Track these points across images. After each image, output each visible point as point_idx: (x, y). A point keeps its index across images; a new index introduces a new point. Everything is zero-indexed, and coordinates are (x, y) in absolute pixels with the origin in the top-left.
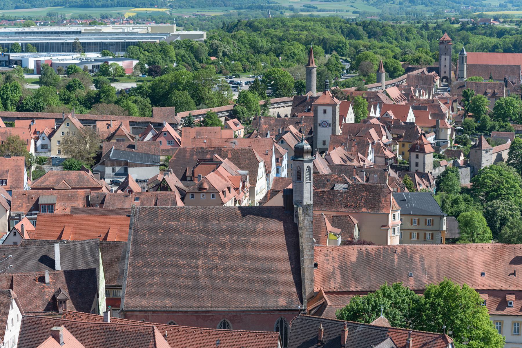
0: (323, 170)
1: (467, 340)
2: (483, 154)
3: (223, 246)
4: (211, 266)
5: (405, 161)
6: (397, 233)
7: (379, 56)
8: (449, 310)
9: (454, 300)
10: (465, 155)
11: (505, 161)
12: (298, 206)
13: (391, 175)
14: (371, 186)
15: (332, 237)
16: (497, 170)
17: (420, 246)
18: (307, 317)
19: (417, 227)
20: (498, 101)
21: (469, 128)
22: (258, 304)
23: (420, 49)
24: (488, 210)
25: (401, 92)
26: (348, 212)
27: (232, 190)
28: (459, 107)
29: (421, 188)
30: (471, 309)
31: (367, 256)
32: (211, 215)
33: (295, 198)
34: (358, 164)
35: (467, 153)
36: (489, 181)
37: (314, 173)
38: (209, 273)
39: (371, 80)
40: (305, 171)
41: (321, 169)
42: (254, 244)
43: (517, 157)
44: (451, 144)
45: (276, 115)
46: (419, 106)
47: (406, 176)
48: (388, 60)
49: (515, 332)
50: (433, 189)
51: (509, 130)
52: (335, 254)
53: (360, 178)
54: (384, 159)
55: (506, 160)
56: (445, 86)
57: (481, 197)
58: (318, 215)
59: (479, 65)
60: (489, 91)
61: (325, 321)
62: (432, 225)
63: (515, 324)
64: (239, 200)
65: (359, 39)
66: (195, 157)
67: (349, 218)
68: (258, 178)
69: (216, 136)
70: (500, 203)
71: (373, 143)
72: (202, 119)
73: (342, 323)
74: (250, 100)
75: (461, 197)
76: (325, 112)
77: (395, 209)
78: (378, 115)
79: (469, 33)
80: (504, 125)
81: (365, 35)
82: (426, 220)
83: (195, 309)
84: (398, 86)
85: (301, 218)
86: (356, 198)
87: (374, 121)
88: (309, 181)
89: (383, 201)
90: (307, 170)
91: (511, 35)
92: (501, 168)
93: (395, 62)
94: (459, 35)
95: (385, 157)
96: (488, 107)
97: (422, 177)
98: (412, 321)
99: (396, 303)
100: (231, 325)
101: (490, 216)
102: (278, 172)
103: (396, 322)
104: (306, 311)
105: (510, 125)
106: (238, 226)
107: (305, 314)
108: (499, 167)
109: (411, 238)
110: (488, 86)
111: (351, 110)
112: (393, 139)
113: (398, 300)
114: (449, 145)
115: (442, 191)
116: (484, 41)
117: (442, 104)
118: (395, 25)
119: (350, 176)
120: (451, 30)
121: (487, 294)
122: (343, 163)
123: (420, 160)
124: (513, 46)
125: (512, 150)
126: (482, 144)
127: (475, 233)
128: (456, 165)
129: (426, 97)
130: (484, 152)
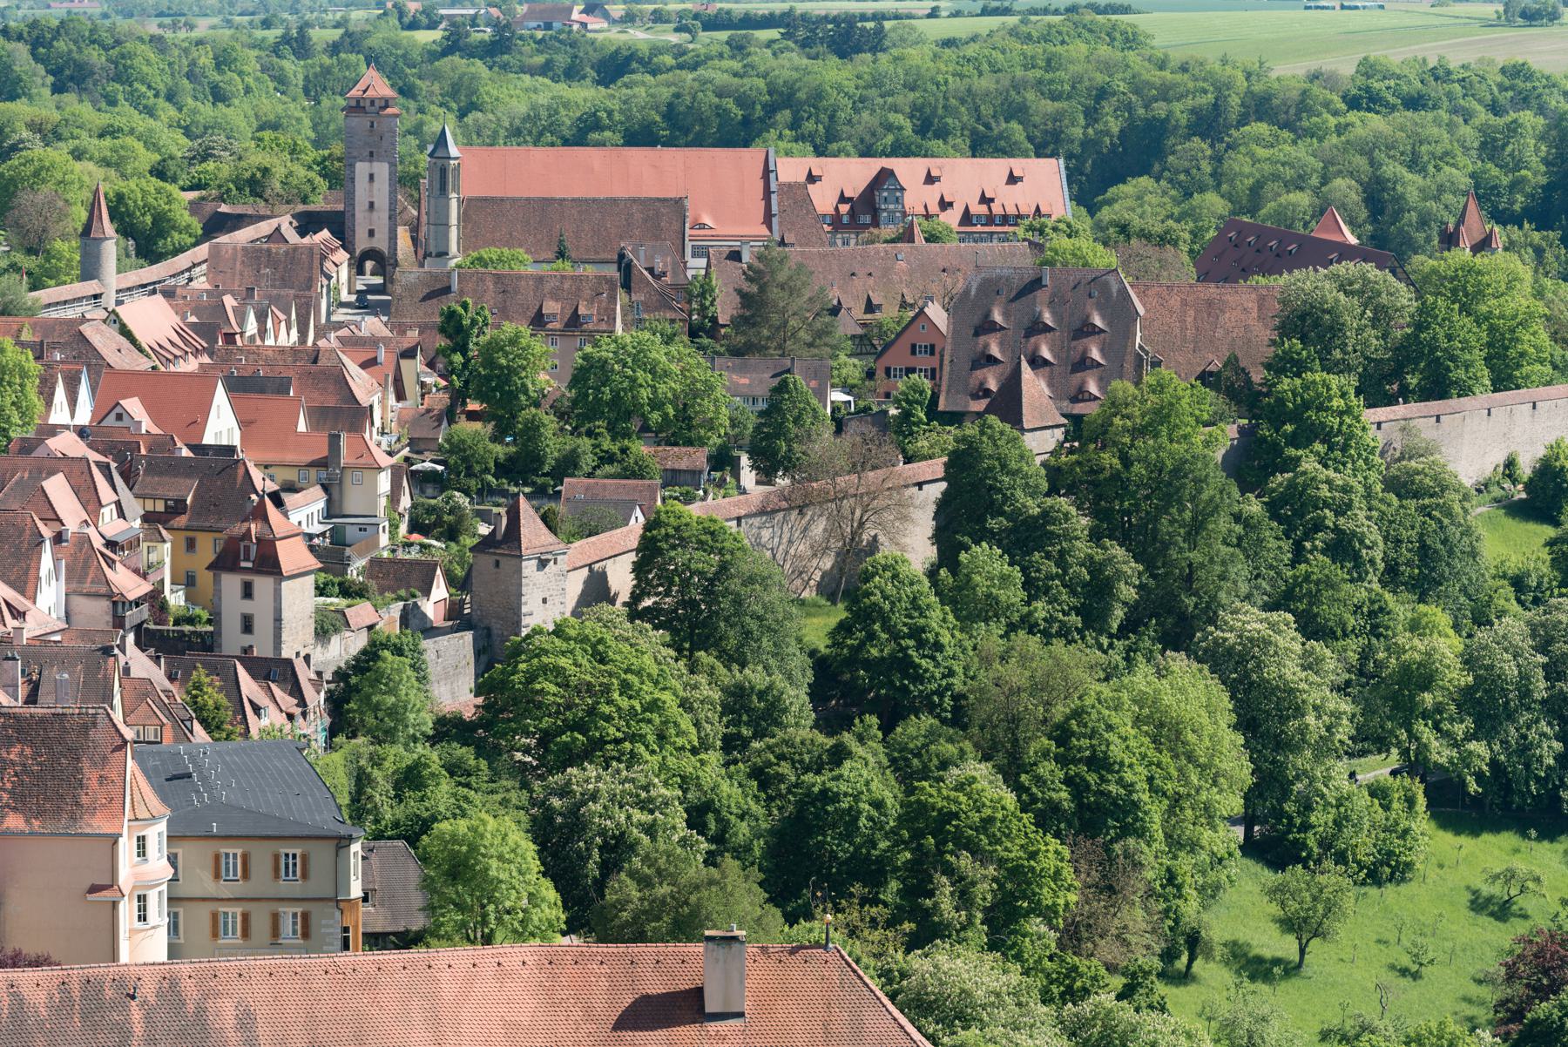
2: (525, 572)
5: (198, 611)
7: (91, 166)
10: (451, 580)
14: (43, 720)
16: (583, 639)
17: (235, 963)
19: (239, 888)
21: (469, 468)
23: (267, 135)
25: (184, 318)
28: (428, 380)
29: (265, 722)
35: (459, 572)
36: (553, 688)
39: (58, 270)
43: (672, 583)
44: (393, 535)
47: (200, 674)
48: (131, 187)
50: (315, 726)
51: (636, 472)
54: (105, 604)
55: (624, 596)
56: (372, 289)
57: (518, 756)
59: (514, 200)
60: (551, 307)
62: (305, 876)
65: (13, 97)
71: (58, 539)
75: (434, 757)
78: (84, 416)
79: (479, 67)
80: (615, 448)
81: (39, 79)
84: (169, 294)
87: (66, 444)
89: (94, 783)
91: (654, 73)
93: (158, 191)
94: (436, 76)
96: (546, 375)
97: (267, 678)
101: (558, 840)
105: (641, 448)
108: (592, 628)
109: (215, 935)
110: (548, 287)
112: (148, 518)
114: (384, 540)
115: (354, 736)
116: (543, 99)
118: (169, 35)
120: (404, 56)
123: (260, 607)
124: (664, 117)
125: (649, 554)
126: (525, 531)
127: (491, 908)
128: (414, 622)
129: (287, 338)
130: (529, 567)
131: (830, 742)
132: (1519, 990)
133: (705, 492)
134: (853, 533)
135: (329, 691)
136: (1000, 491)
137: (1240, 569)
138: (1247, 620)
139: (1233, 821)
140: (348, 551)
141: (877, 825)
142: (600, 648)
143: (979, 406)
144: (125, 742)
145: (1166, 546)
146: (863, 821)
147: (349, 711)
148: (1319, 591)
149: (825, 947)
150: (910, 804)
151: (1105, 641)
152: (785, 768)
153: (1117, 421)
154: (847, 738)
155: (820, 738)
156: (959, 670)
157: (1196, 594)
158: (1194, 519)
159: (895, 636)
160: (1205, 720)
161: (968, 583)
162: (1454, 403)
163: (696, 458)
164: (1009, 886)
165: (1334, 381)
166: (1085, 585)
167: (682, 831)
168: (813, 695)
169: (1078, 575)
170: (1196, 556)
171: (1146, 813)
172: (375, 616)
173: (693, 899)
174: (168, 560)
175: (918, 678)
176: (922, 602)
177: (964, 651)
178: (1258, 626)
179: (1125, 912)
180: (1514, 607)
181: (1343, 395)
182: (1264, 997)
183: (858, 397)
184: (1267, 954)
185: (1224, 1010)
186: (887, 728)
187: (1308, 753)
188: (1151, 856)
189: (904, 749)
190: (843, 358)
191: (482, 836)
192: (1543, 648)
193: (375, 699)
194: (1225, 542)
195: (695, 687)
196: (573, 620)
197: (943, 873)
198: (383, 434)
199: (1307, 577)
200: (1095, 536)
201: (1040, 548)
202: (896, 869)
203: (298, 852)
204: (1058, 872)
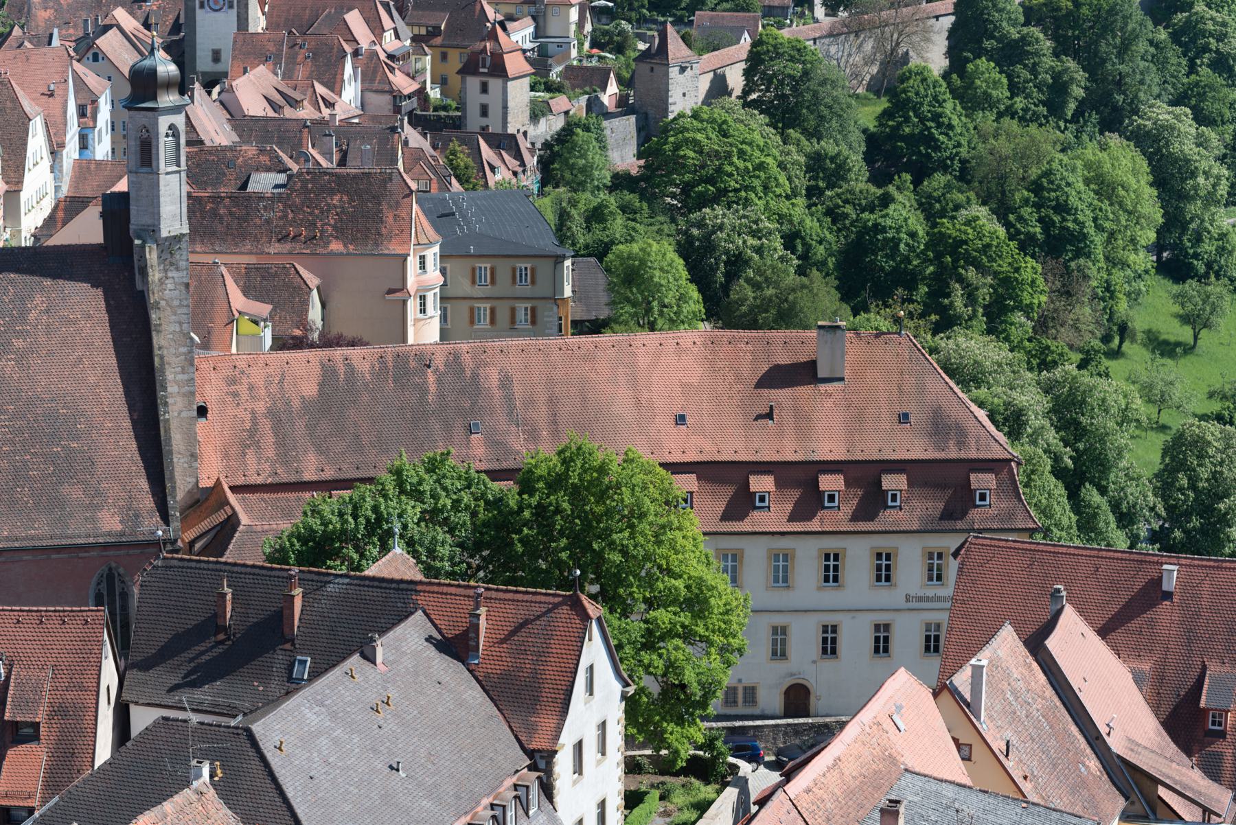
0: (213, 134)
1: (643, 607)
2: (671, 75)
5: (449, 101)
6: (433, 310)
8: (587, 526)
9: (602, 496)
10: (620, 81)
11: (735, 94)
12: (144, 242)
13: (412, 144)
14: (355, 177)
15: (246, 327)
16: (712, 121)
17: (497, 343)
18: (181, 560)
19: (488, 291)
22: (39, 530)
26: (290, 253)
29: (498, 177)
30: (651, 518)
31: (347, 379)
33: (137, 219)
35: (627, 75)
36: (692, 154)
37: (189, 143)
41: (208, 132)
43: (770, 82)
44: (579, 51)
47: (455, 145)
49: (776, 580)
50: (531, 180)
52: (257, 376)
53: (323, 154)
54: (388, 98)
55: (738, 92)
58: (203, 265)
61: (237, 572)
62: (533, 282)
63: (777, 556)
67: (292, 271)
68: (29, 163)
70: (724, 215)
71: (356, 53)
73: (285, 574)
75: (612, 201)
77: (423, 240)
82: (514, 270)
85: (155, 275)
86: (311, 214)
88: (176, 169)
89: (391, 220)
90: (167, 136)
95: (391, 91)
97: (498, 147)
98: (483, 559)
99: (436, 511)
101: (696, 255)
102: (84, 144)
103: (438, 564)
104: (180, 543)
107: (177, 551)
108: (718, 113)
109: (472, 322)
112: (415, 39)
113: (441, 502)
114: (574, 53)
115: (557, 186)
119: (293, 149)
121: (694, 476)
122: (271, 113)
123: (493, 99)
125: (755, 62)
126: (670, 47)
127: (655, 303)
128: (595, 108)
130: (674, 72)
131: (880, 192)
133: (791, 21)
134: (893, 50)
135: (540, 157)
136: (992, 22)
137: (1153, 77)
138: (1162, 113)
140: (550, 61)
142: (724, 127)
144: (412, 192)
145: (1104, 61)
146: (902, 246)
147: (554, 169)
148: (1205, 93)
149: (899, 334)
150: (934, 234)
151: (1062, 124)
152: (849, 209)
154: (891, 189)
155: (873, 189)
156: (964, 142)
157: (1124, 94)
158: (1122, 43)
159: (922, 120)
160: (1133, 181)
161: (970, 85)
164: (1000, 290)
166: (1049, 87)
167: (781, 251)
168: (865, 159)
169: (1045, 80)
171: (1091, 242)
173: (791, 298)
174: (429, 67)
175: (937, 148)
176: (941, 98)
177: (968, 130)
178: (1167, 117)
179: (1077, 310)
182: (1170, 369)
184: (1172, 339)
185: (1144, 378)
186: (917, 182)
187: (1199, 202)
188: (1096, 271)
189: (929, 196)
191: (649, 254)
193: (571, 161)
194: (1143, 58)
195: (788, 154)
196: (705, 107)
197: (957, 281)
199: (1197, 84)
201: (1020, 62)
202: (924, 278)
203: (529, 266)
204: (1033, 282)
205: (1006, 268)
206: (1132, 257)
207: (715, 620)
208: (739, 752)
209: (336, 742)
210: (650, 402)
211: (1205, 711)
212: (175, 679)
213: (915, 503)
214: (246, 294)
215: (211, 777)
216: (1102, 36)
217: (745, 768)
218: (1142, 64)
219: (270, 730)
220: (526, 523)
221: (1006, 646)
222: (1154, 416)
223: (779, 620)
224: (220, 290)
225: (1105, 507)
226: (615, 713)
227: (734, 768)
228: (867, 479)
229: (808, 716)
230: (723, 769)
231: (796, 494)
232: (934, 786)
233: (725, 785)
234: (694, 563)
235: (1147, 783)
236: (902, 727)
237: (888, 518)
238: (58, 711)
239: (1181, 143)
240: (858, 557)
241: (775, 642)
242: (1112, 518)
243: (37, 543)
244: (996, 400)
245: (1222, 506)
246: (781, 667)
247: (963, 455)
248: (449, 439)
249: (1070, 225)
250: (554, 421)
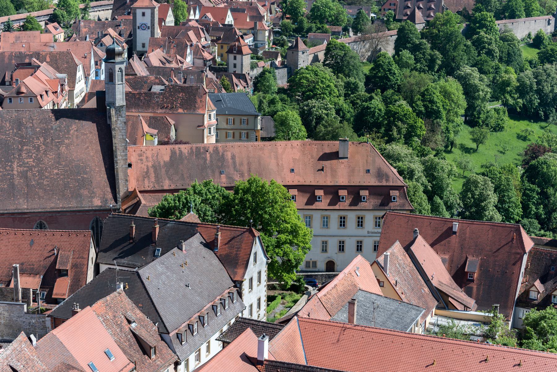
1: (276, 233)
3: (38, 149)
4: (25, 169)
5: (223, 62)
6: (213, 133)
8: (257, 205)
9: (263, 196)
10: (282, 56)
12: (110, 108)
14: (187, 87)
15: (149, 137)
16: (312, 70)
17: (231, 144)
20: (315, 3)
22: (73, 205)
24: (304, 109)
27: (50, 93)
28: (277, 10)
30: (279, 203)
31: (179, 155)
32: (25, 118)
33: (108, 99)
34: (177, 66)
35: (284, 54)
36: (305, 82)
37: (126, 75)
38: (23, 175)
40: (117, 73)
41: (138, 71)
42: (68, 146)
43: (333, 58)
45: (96, 18)
46: (237, 8)
49: (324, 226)
50: (250, 90)
51: (326, 32)
52: (149, 154)
54: (202, 61)
57: (297, 97)
58: (134, 116)
62: (247, 124)
63: (324, 217)
64: (58, 104)
66: (13, 61)
68: (77, 81)
69: (35, 41)
70: (315, 103)
71: (191, 45)
72: (22, 24)
74: (70, 4)
75: (277, 97)
76: (144, 14)
78: (197, 17)
80: (320, 26)
82: (241, 120)
83: (11, 212)
85: (114, 119)
86: (172, 99)
87: (193, 24)
92: (316, 69)
95: (203, 59)
97: (239, 78)
100: (47, 226)
102: (97, 75)
103: (207, 218)
104: (121, 210)
105: (327, 26)
106: (52, 129)
107: (120, 212)
108: (315, 68)
109: (226, 137)
111: (170, 12)
112: (212, 41)
113: (208, 197)
114: (267, 47)
117: (260, 7)
122: (162, 65)
123: (238, 62)
125: (328, 50)
128: (273, 66)
130: (300, 54)
131: (369, 95)
132: (528, 157)
134: (376, 47)
137: (465, 57)
138: (467, 69)
139: (462, 116)
141: (379, 115)
143: (405, 18)
146: (376, 114)
151: (433, 73)
152: (358, 101)
153: (438, 22)
154: (373, 94)
155: (367, 94)
156: (399, 79)
157: (455, 63)
160: (456, 92)
162: (516, 20)
163: (340, 29)
165: (488, 14)
166: (429, 60)
167: (334, 115)
170: (455, 54)
172: (265, 64)
173: (337, 131)
180: (529, 68)
181: (490, 17)
183: (377, 15)
184: (469, 147)
185: (459, 160)
187: (480, 101)
188: (443, 123)
189: (386, 97)
190: (374, 6)
192: (536, 78)
194: (462, 51)
195: (338, 82)
198: (267, 22)
199: (481, 60)
200: (432, 49)
202: (384, 125)
204: (421, 127)
205: (412, 122)
206: (456, 119)
207: (300, 239)
208: (309, 283)
209: (168, 277)
210: (282, 164)
211: (467, 273)
212: (116, 256)
213: (371, 200)
214: (149, 126)
215: (124, 288)
216: (448, 43)
217: (311, 288)
218: (462, 53)
219: (144, 272)
220: (237, 205)
221: (397, 248)
222: (462, 173)
223: (324, 239)
224: (140, 125)
225: (442, 203)
226: (264, 269)
227: (307, 288)
228: (355, 192)
229: (334, 271)
230: (303, 289)
231: (331, 197)
232: (368, 295)
233: (304, 294)
234: (294, 219)
235: (445, 297)
236: (359, 275)
237: (362, 205)
238: (74, 266)
239: (474, 80)
240: (352, 217)
241: (323, 246)
242: (444, 207)
243: (72, 209)
244: (405, 167)
245: (483, 204)
246: (325, 255)
247: (388, 184)
248: (214, 176)
249: (434, 107)
250: (249, 171)
